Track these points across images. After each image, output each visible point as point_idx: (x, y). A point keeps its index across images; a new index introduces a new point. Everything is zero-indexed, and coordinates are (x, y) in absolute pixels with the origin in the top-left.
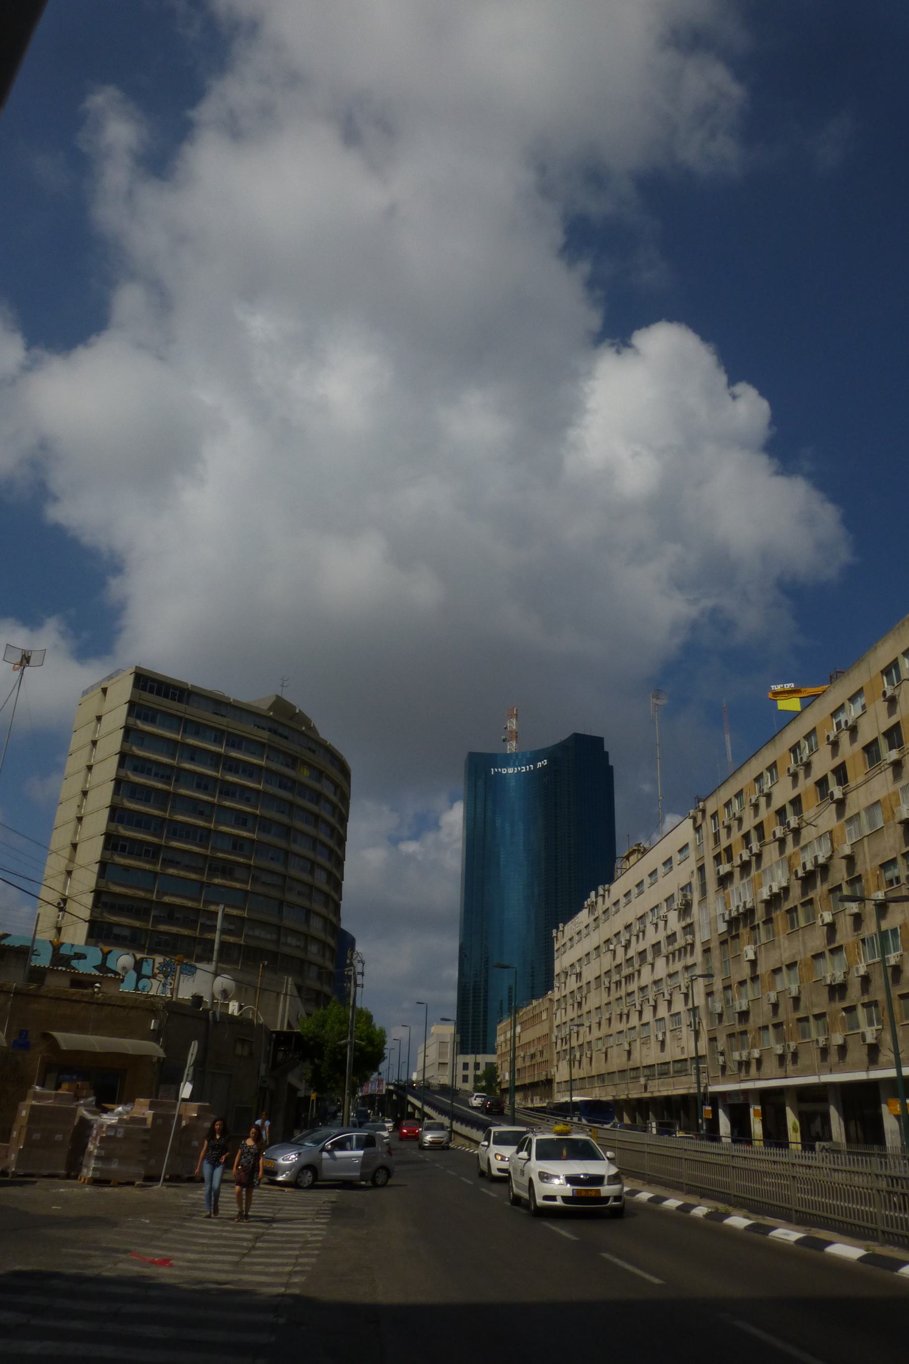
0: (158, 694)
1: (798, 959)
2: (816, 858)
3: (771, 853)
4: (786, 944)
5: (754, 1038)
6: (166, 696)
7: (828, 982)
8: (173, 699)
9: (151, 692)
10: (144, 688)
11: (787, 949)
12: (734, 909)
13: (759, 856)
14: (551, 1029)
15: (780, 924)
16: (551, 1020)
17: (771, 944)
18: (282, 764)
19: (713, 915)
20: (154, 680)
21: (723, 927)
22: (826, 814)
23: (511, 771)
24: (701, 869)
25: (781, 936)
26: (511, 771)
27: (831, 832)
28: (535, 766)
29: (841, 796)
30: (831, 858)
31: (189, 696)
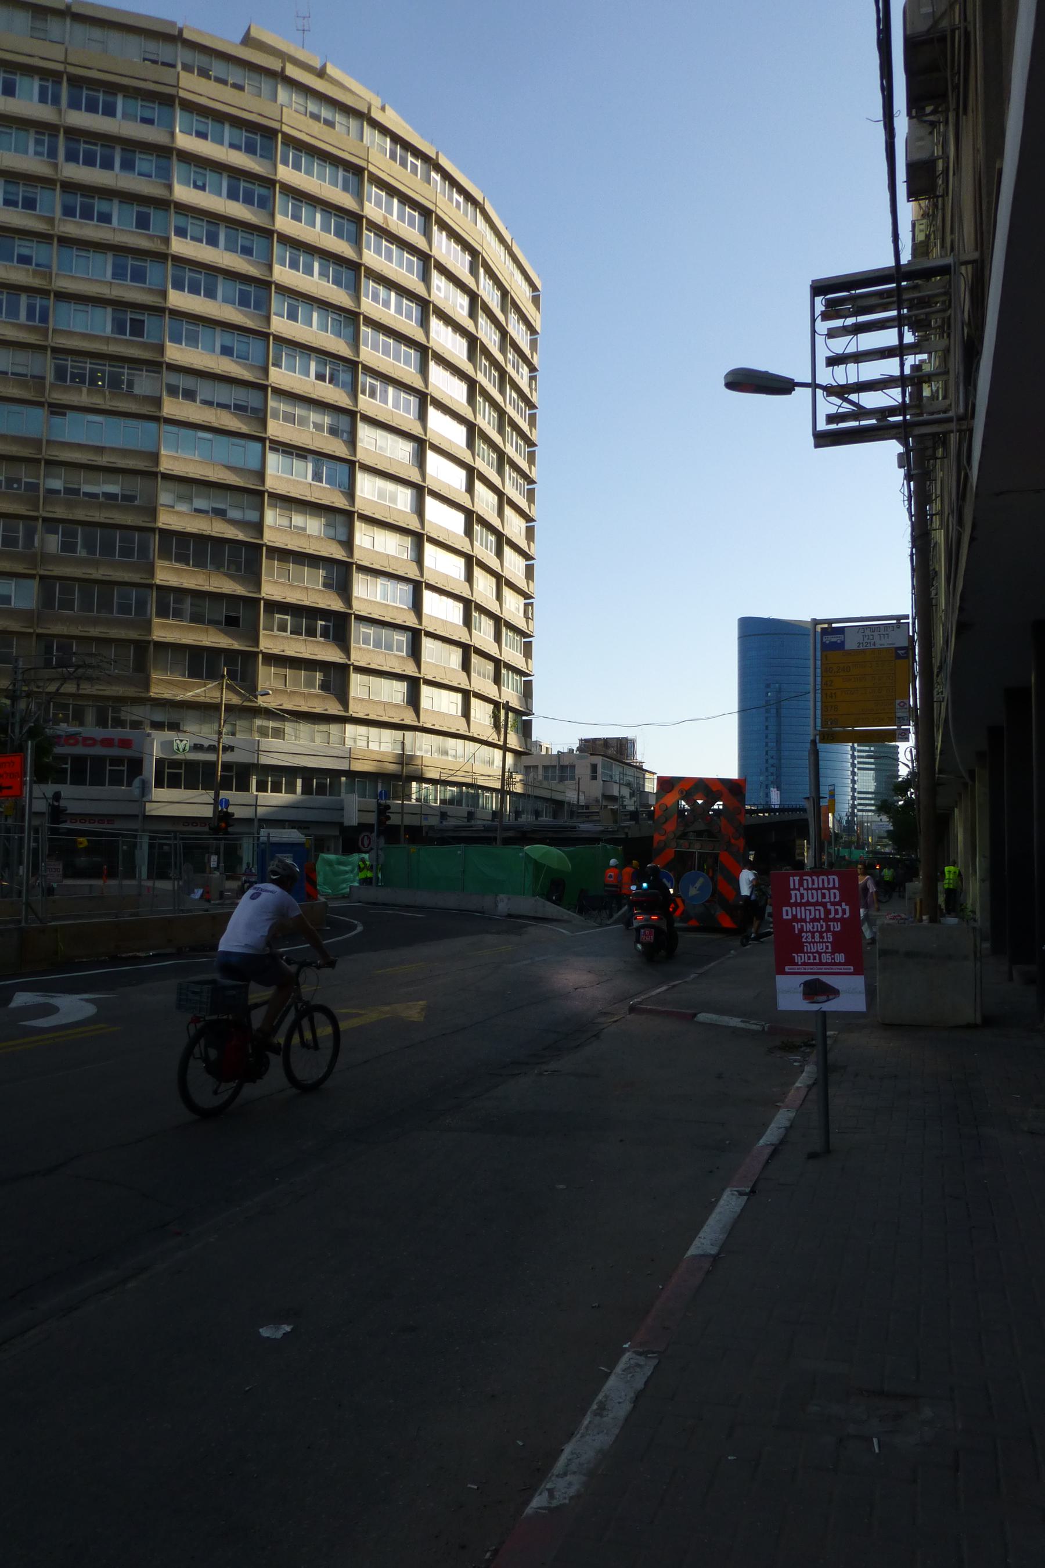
18: (232, 146)
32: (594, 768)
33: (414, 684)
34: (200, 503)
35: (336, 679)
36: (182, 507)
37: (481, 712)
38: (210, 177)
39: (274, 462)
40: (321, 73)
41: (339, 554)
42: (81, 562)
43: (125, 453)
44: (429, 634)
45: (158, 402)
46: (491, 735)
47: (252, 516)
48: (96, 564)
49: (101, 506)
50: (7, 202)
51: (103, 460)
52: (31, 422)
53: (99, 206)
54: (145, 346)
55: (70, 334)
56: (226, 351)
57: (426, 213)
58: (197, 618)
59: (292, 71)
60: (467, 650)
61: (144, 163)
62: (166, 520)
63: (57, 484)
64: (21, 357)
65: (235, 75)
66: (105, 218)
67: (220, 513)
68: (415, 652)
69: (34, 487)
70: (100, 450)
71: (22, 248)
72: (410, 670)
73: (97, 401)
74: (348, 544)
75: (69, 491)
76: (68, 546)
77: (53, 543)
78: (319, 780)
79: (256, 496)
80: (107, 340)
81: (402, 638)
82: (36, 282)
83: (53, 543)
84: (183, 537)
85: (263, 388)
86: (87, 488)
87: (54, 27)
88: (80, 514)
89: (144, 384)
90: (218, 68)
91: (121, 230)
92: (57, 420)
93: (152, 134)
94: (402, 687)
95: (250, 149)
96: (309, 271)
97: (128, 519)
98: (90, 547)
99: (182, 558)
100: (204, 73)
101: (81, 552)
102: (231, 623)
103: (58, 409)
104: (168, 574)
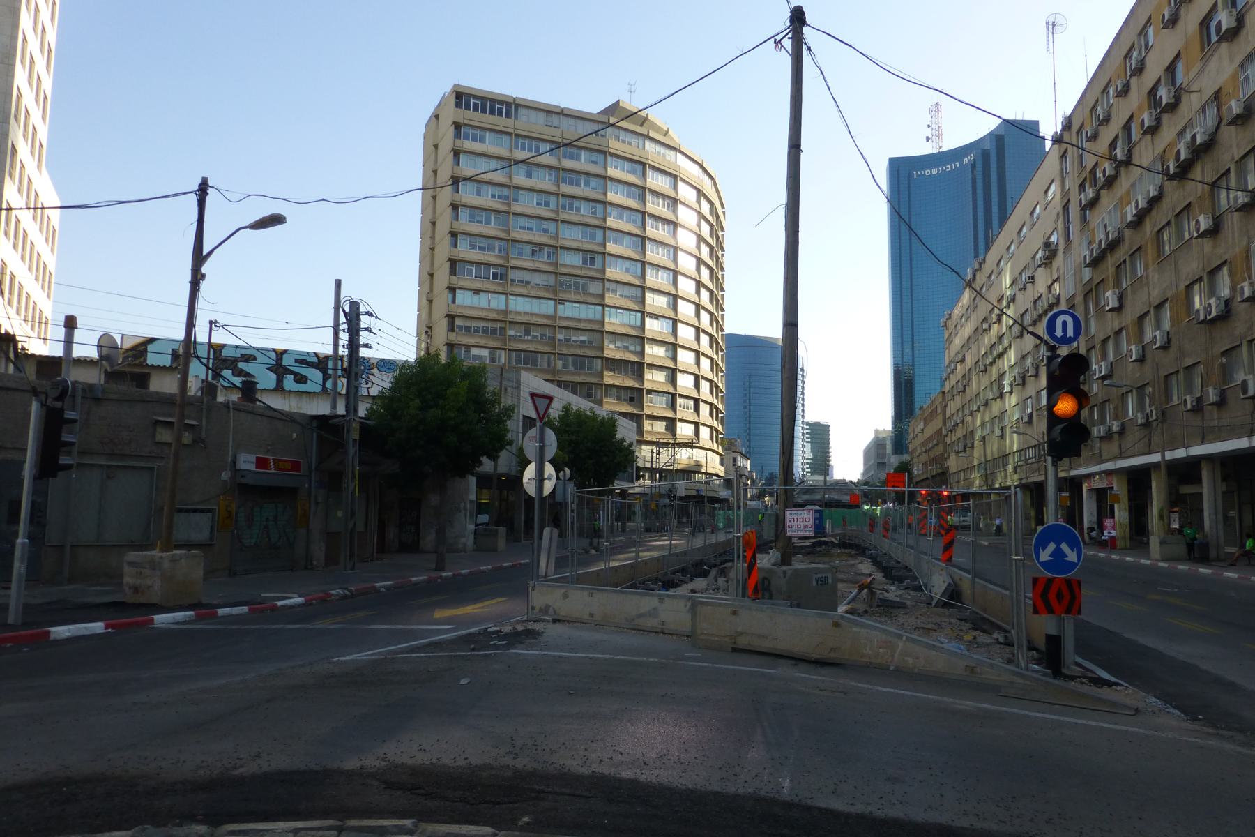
0: (484, 111)
1: (1169, 294)
2: (1194, 137)
3: (1146, 154)
4: (1157, 276)
5: (1116, 408)
6: (492, 112)
7: (1202, 318)
8: (500, 114)
9: (476, 109)
10: (468, 107)
11: (1159, 284)
12: (1095, 246)
13: (1128, 162)
14: (944, 424)
15: (1150, 251)
16: (944, 414)
17: (1140, 283)
19: (1078, 262)
20: (476, 97)
21: (1087, 274)
22: (1213, 64)
23: (935, 171)
24: (1066, 208)
25: (1150, 270)
26: (935, 171)
27: (1217, 94)
28: (961, 163)
29: (1234, 24)
30: (1218, 128)
31: (516, 110)
32: (735, 460)
33: (697, 425)
34: (619, 344)
35: (671, 424)
36: (612, 346)
37: (705, 432)
38: (620, 186)
39: (649, 322)
40: (666, 134)
41: (672, 366)
42: (572, 373)
43: (590, 321)
44: (682, 396)
45: (603, 297)
46: (708, 444)
47: (638, 348)
48: (579, 374)
49: (580, 347)
50: (538, 204)
51: (581, 325)
52: (547, 307)
53: (576, 203)
54: (597, 270)
55: (566, 266)
56: (628, 270)
57: (698, 191)
58: (618, 399)
59: (652, 134)
60: (697, 401)
61: (594, 182)
62: (608, 353)
63: (560, 336)
64: (544, 276)
65: (628, 137)
66: (578, 209)
67: (626, 348)
68: (673, 406)
69: (554, 338)
70: (580, 320)
71: (545, 225)
72: (670, 414)
73: (578, 297)
74: (674, 358)
75: (567, 340)
76: (565, 366)
77: (560, 364)
78: (665, 473)
79: (642, 340)
80: (581, 268)
81: (691, 403)
82: (551, 242)
83: (560, 364)
84: (613, 360)
85: (643, 288)
86: (574, 338)
87: (555, 120)
88: (572, 351)
89: (594, 288)
90: (623, 135)
91: (584, 212)
92: (560, 307)
93: (600, 171)
94: (692, 427)
95: (635, 173)
96: (657, 229)
97: (593, 353)
98: (575, 364)
99: (613, 370)
100: (617, 138)
101: (571, 369)
102: (632, 399)
103: (562, 302)
104: (610, 378)
